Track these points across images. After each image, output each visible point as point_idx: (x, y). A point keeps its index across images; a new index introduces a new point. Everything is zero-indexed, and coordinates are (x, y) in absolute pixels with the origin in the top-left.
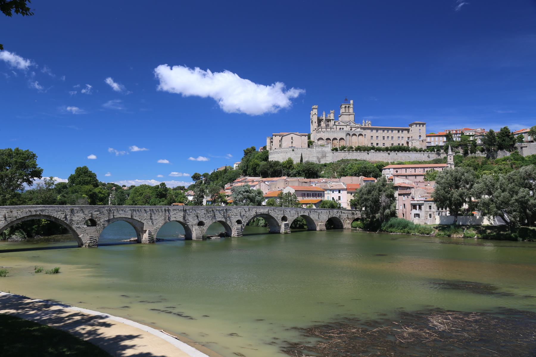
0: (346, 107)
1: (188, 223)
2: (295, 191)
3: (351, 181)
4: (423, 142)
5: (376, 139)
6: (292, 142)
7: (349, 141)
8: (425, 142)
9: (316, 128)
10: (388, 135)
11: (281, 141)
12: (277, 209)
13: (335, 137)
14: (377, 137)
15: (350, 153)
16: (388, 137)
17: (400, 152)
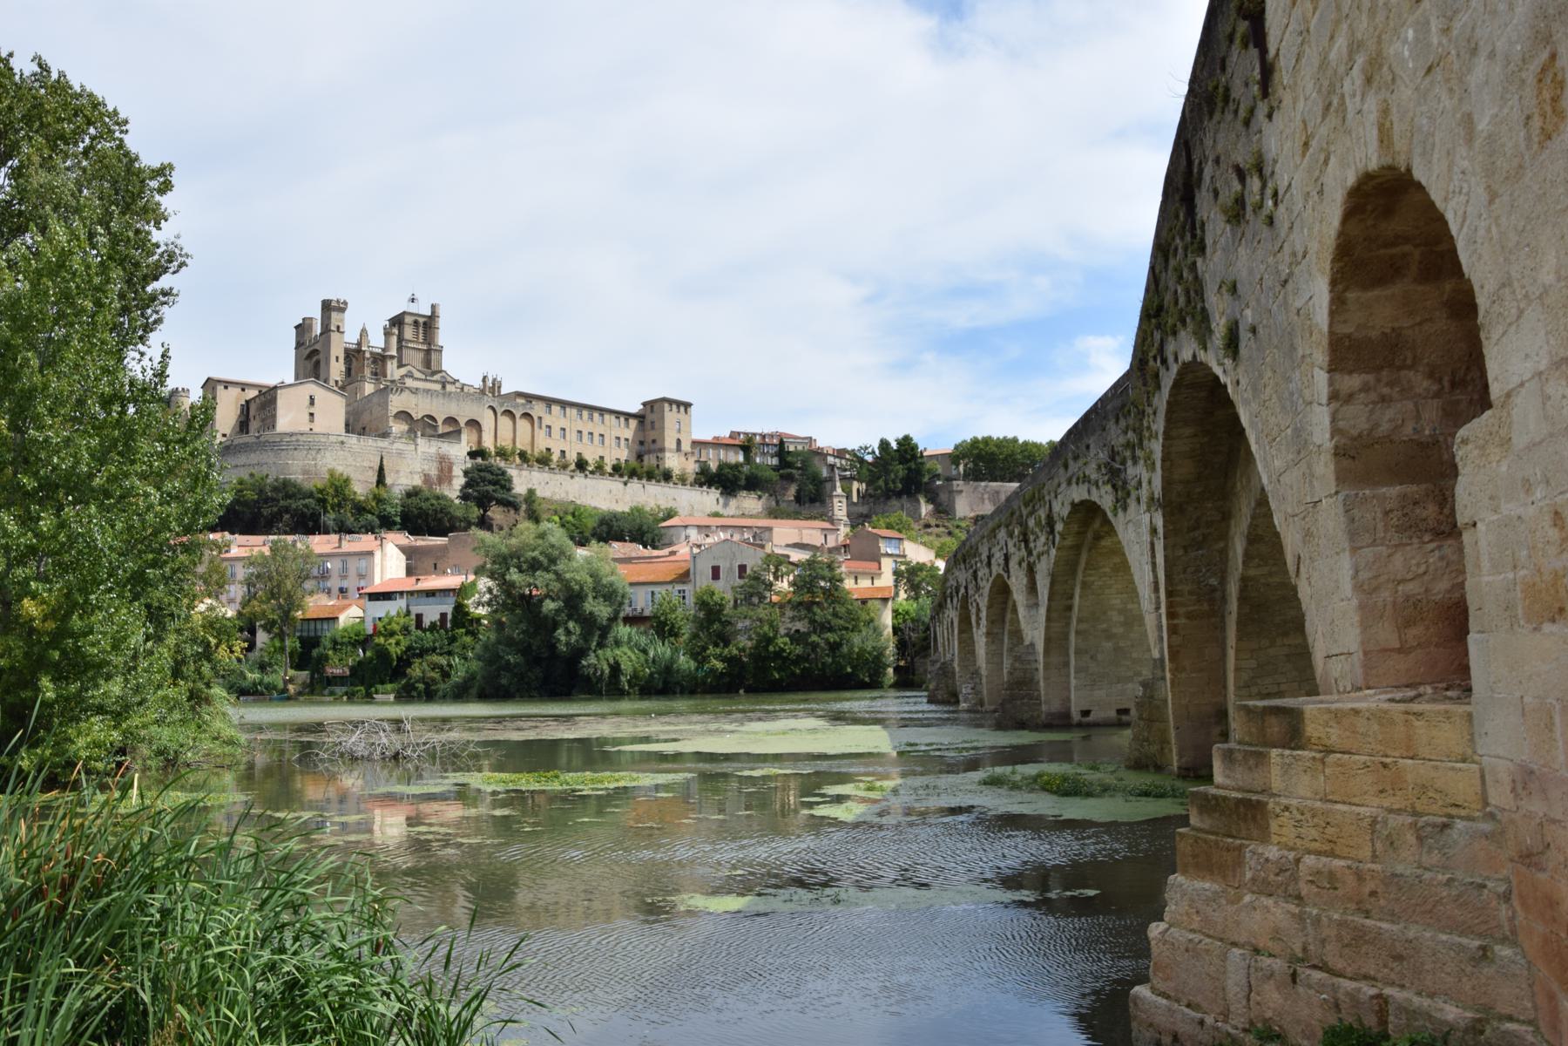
0: (416, 322)
6: (312, 414)
14: (564, 429)
15: (525, 473)
17: (654, 482)
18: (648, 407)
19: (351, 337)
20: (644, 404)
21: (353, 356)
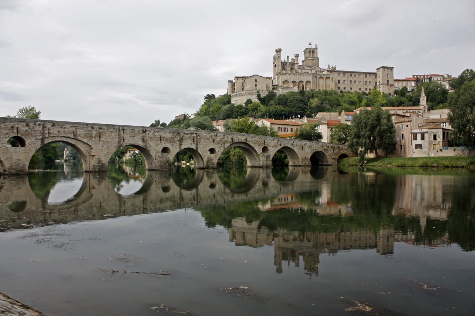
0: (310, 51)
1: (149, 148)
2: (271, 124)
3: (330, 117)
4: (391, 87)
5: (343, 83)
7: (316, 84)
8: (393, 87)
9: (280, 72)
10: (355, 79)
11: (243, 85)
12: (257, 137)
13: (302, 79)
14: (345, 81)
16: (355, 81)
18: (378, 70)
19: (283, 58)
20: (377, 69)
21: (284, 64)
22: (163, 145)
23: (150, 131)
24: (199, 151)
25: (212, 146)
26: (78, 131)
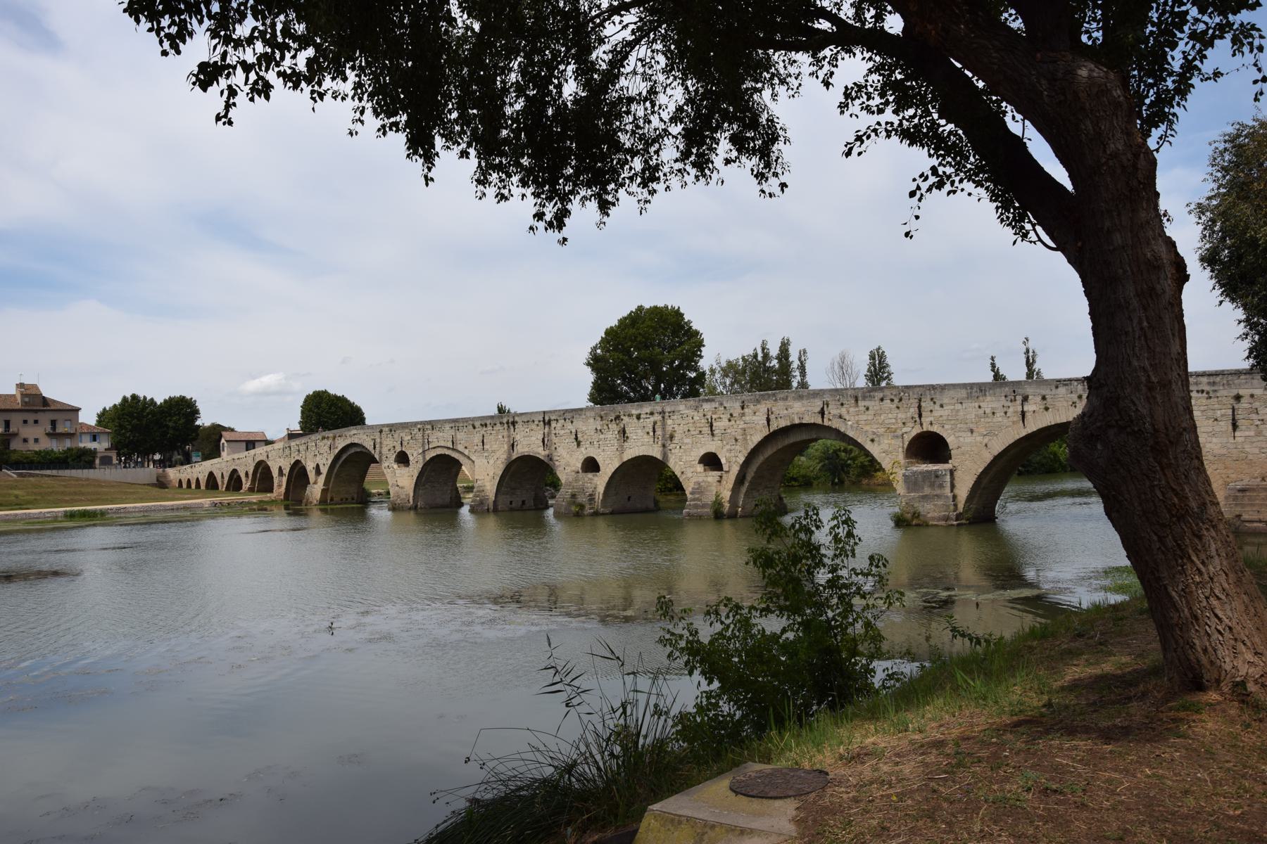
22: (584, 452)
23: (557, 420)
24: (671, 464)
25: (711, 446)
26: (458, 433)
